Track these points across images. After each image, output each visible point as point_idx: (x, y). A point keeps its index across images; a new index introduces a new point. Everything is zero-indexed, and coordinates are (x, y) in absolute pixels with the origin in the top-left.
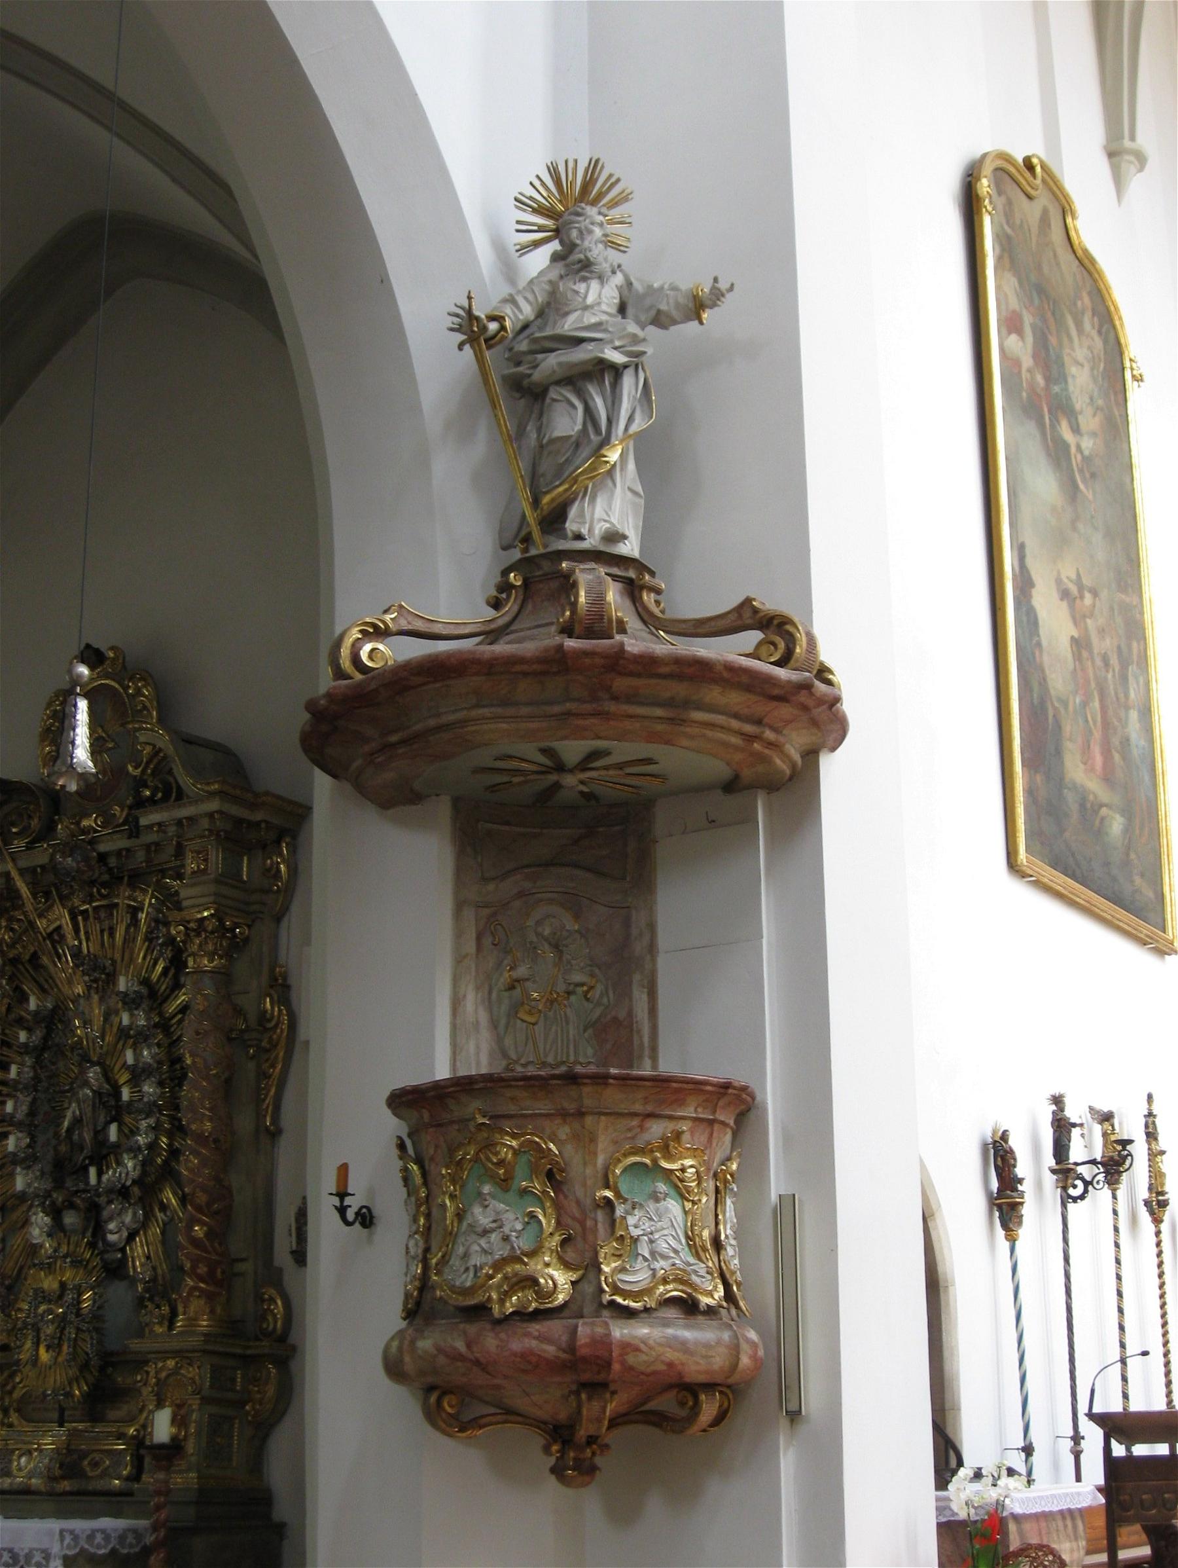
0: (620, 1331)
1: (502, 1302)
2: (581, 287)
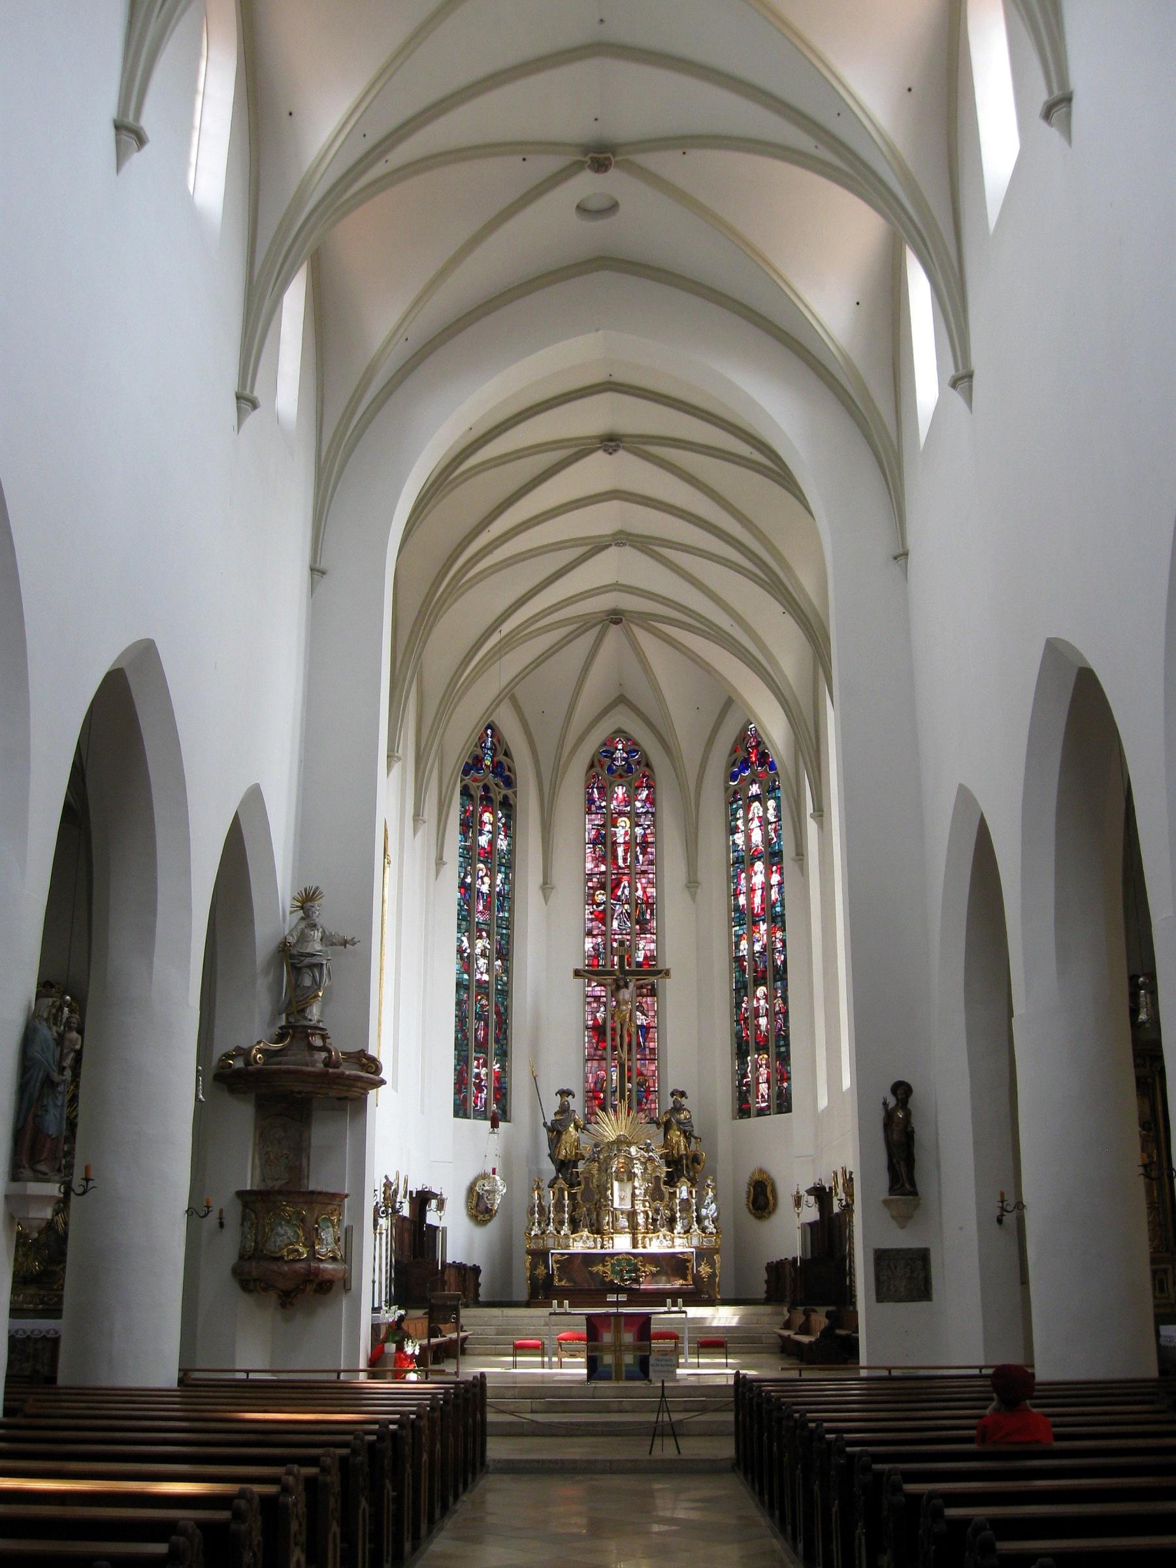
0: (322, 1266)
1: (288, 1255)
2: (312, 933)
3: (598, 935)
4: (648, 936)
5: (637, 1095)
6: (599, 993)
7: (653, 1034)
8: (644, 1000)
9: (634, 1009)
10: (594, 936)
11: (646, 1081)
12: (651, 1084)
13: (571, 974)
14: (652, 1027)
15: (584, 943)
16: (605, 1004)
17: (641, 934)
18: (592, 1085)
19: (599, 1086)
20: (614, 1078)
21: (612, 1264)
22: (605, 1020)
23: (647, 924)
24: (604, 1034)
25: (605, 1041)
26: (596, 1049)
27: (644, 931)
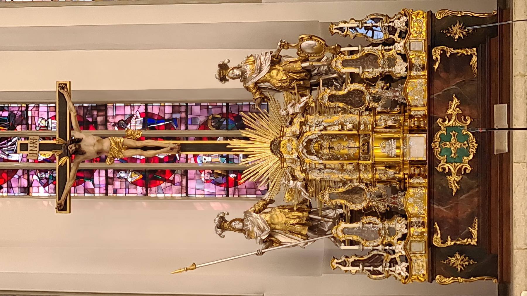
3: (28, 179)
4: (30, 114)
5: (232, 129)
6: (103, 179)
7: (154, 109)
8: (111, 120)
9: (123, 132)
10: (30, 184)
11: (214, 118)
12: (218, 110)
13: (63, 214)
14: (146, 109)
15: (38, 197)
16: (117, 171)
17: (27, 124)
18: (218, 188)
19: (220, 179)
20: (209, 159)
21: (447, 162)
22: (137, 171)
23: (15, 115)
24: (154, 171)
25: (163, 171)
26: (173, 182)
27: (23, 120)
